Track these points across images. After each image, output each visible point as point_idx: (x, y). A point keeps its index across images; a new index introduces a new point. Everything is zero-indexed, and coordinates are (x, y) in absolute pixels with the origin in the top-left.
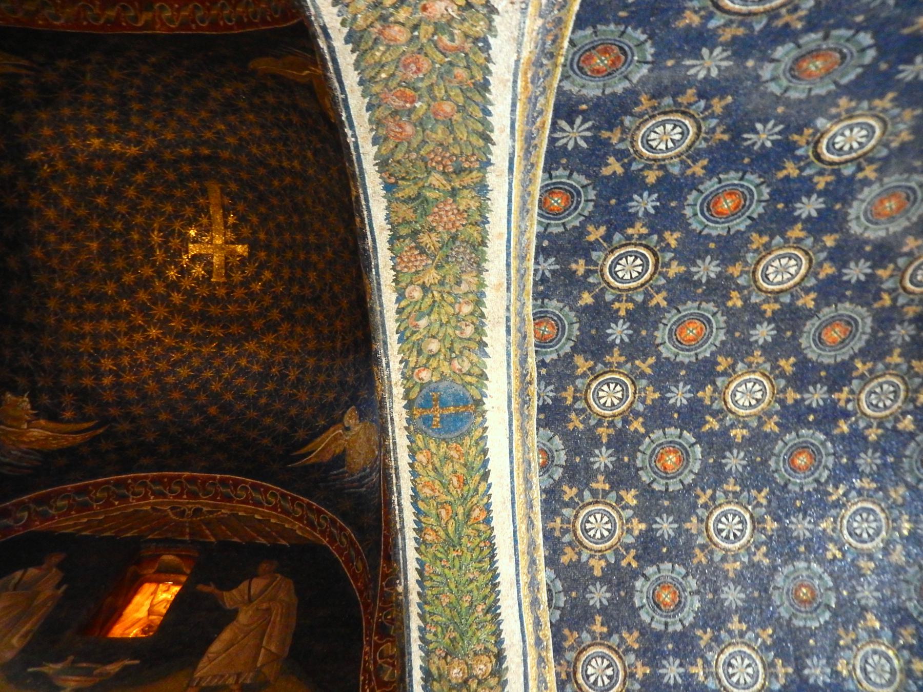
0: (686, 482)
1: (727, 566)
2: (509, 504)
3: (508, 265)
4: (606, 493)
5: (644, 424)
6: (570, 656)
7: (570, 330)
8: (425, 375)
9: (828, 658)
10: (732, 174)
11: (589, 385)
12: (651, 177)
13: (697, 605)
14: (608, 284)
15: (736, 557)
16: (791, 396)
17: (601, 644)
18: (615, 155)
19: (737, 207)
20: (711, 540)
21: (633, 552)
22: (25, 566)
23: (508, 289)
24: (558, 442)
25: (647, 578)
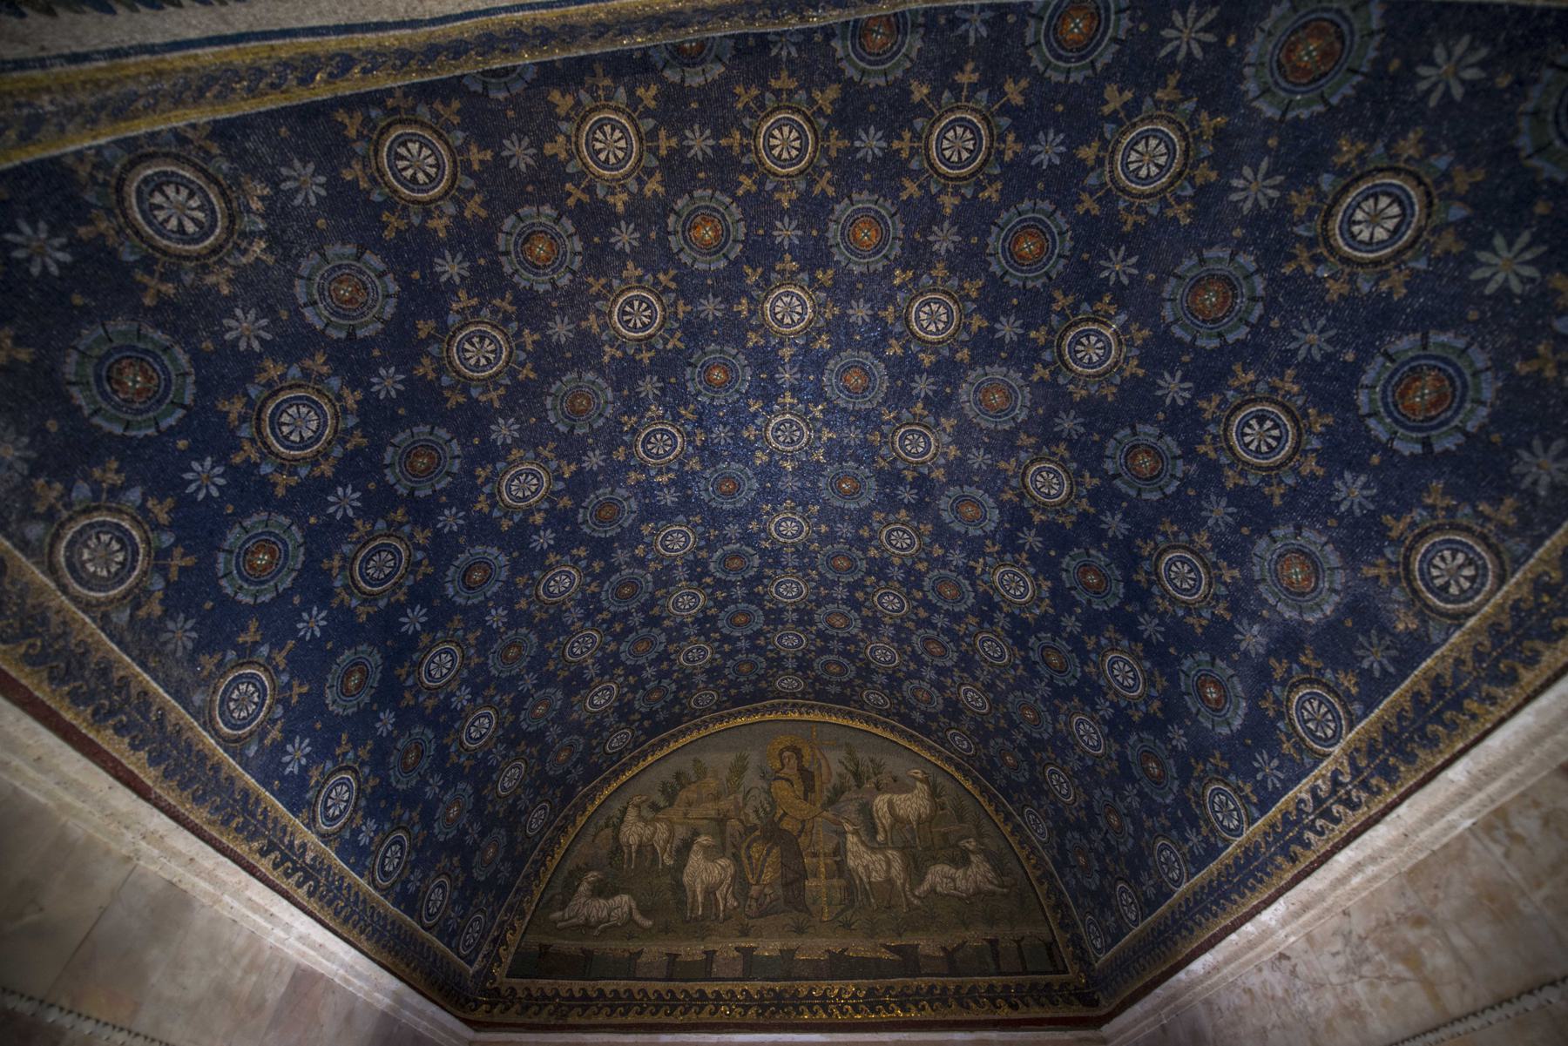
0: (682, 256)
1: (592, 317)
4: (654, 151)
5: (748, 192)
6: (423, 111)
7: (876, 72)
9: (521, 439)
10: (1069, 244)
11: (799, 111)
12: (1087, 153)
13: (541, 289)
14: (939, 119)
15: (604, 327)
16: (787, 352)
17: (455, 162)
19: (1020, 257)
20: (618, 296)
21: (586, 198)
24: (717, 70)
25: (557, 220)
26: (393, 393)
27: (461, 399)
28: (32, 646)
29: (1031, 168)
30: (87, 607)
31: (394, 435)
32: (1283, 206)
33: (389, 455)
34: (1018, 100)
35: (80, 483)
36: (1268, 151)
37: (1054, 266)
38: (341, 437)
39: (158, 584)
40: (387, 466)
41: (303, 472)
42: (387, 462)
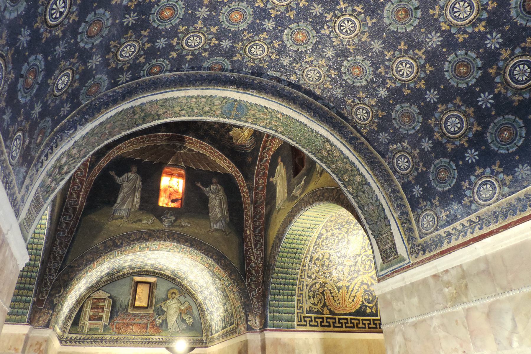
2: (281, 106)
3: (177, 91)
6: (350, 117)
8: (218, 112)
10: (151, 18)
13: (368, 63)
18: (135, 62)
19: (169, 9)
22: (276, 168)
23: (188, 90)
26: (436, 92)
27: (428, 65)
28: (501, 217)
29: (167, 37)
30: (497, 200)
31: (453, 86)
32: (85, 63)
33: (463, 86)
34: (172, 53)
35: (465, 193)
36: (94, 70)
37: (156, 9)
38: (457, 108)
39: (501, 176)
40: (468, 85)
41: (472, 120)
42: (466, 86)
